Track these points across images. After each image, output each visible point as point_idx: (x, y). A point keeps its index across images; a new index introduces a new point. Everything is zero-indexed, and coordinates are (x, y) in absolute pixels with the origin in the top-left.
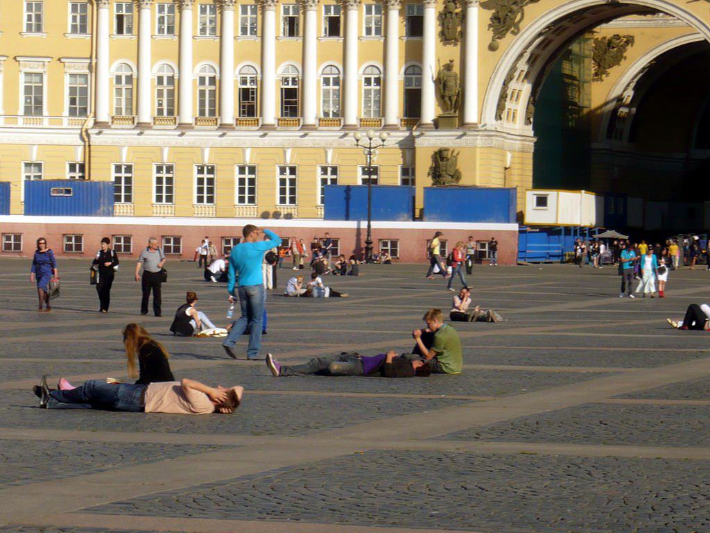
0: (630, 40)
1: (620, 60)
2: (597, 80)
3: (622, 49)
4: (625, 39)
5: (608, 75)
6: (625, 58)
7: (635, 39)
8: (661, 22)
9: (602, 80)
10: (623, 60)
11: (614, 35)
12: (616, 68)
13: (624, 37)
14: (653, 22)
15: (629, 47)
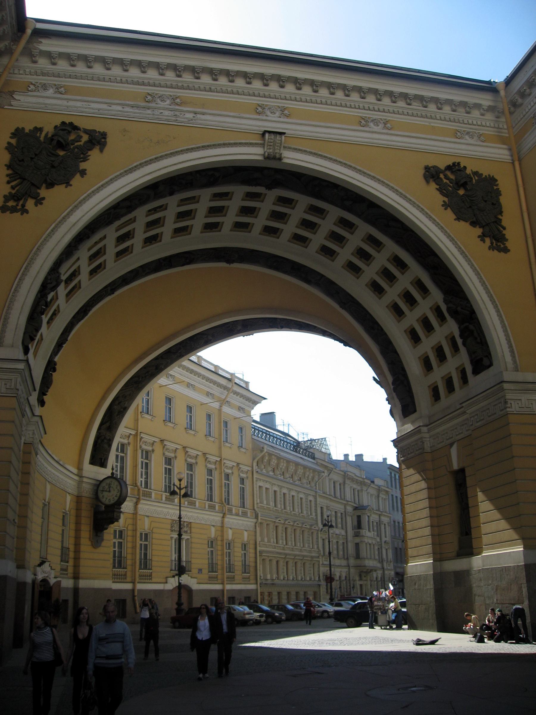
0: (98, 140)
1: (73, 176)
2: (13, 210)
3: (82, 155)
4: (85, 138)
5: (39, 201)
6: (83, 173)
7: (110, 140)
8: (166, 113)
9: (27, 212)
10: (78, 175)
11: (63, 123)
12: (59, 190)
13: (86, 131)
14: (149, 112)
15: (94, 154)
